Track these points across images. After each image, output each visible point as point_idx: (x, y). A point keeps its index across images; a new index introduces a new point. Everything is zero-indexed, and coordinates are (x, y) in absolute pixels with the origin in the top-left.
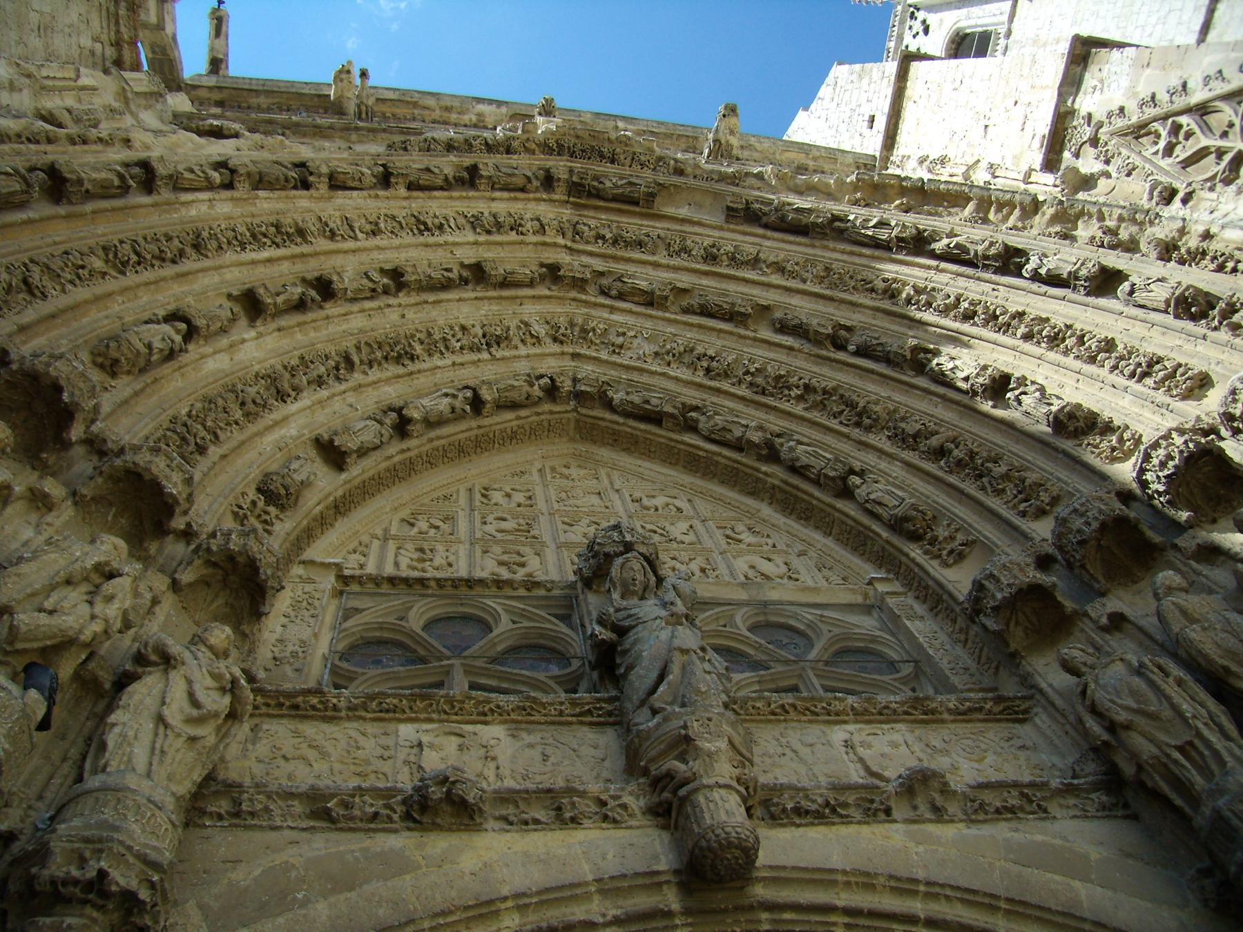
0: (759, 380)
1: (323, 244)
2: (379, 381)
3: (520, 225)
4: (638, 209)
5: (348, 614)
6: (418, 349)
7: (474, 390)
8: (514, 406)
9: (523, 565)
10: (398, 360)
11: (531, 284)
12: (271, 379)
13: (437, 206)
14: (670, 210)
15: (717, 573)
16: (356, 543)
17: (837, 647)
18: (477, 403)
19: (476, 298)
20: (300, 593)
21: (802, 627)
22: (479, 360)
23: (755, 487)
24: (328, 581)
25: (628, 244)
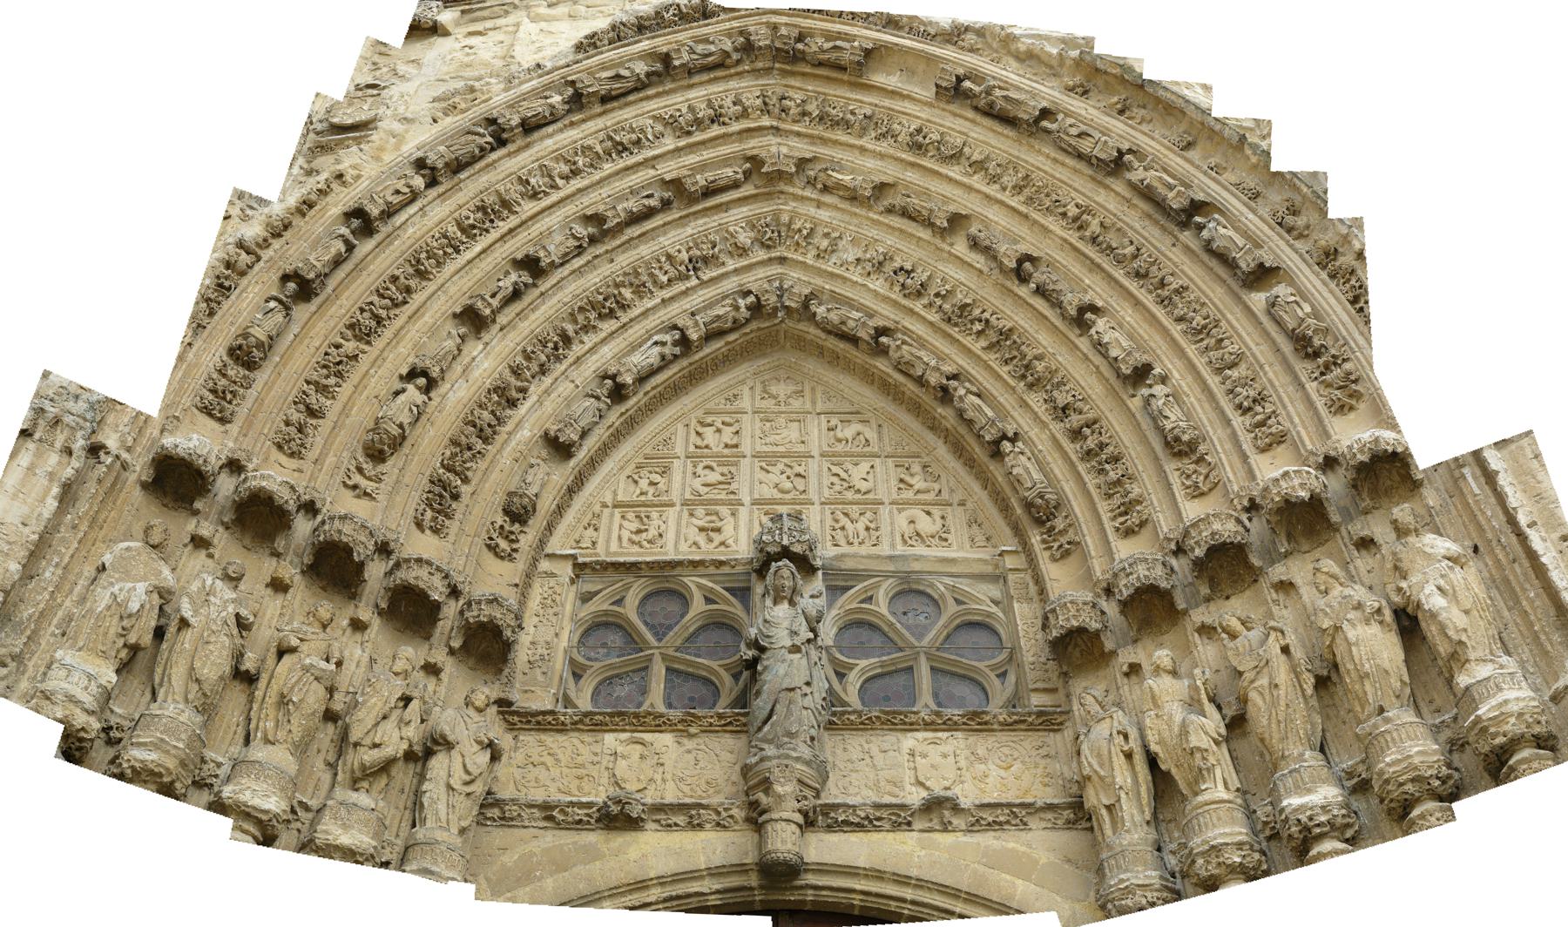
0: (947, 306)
1: (529, 207)
2: (596, 345)
3: (720, 115)
4: (846, 77)
5: (586, 598)
6: (627, 293)
7: (682, 330)
8: (721, 333)
9: (718, 530)
10: (611, 314)
11: (736, 185)
12: (500, 390)
13: (635, 115)
14: (879, 79)
15: (878, 533)
16: (590, 516)
17: (958, 621)
18: (684, 342)
19: (681, 218)
20: (546, 589)
21: (936, 597)
22: (687, 289)
23: (934, 426)
24: (566, 570)
25: (836, 124)
